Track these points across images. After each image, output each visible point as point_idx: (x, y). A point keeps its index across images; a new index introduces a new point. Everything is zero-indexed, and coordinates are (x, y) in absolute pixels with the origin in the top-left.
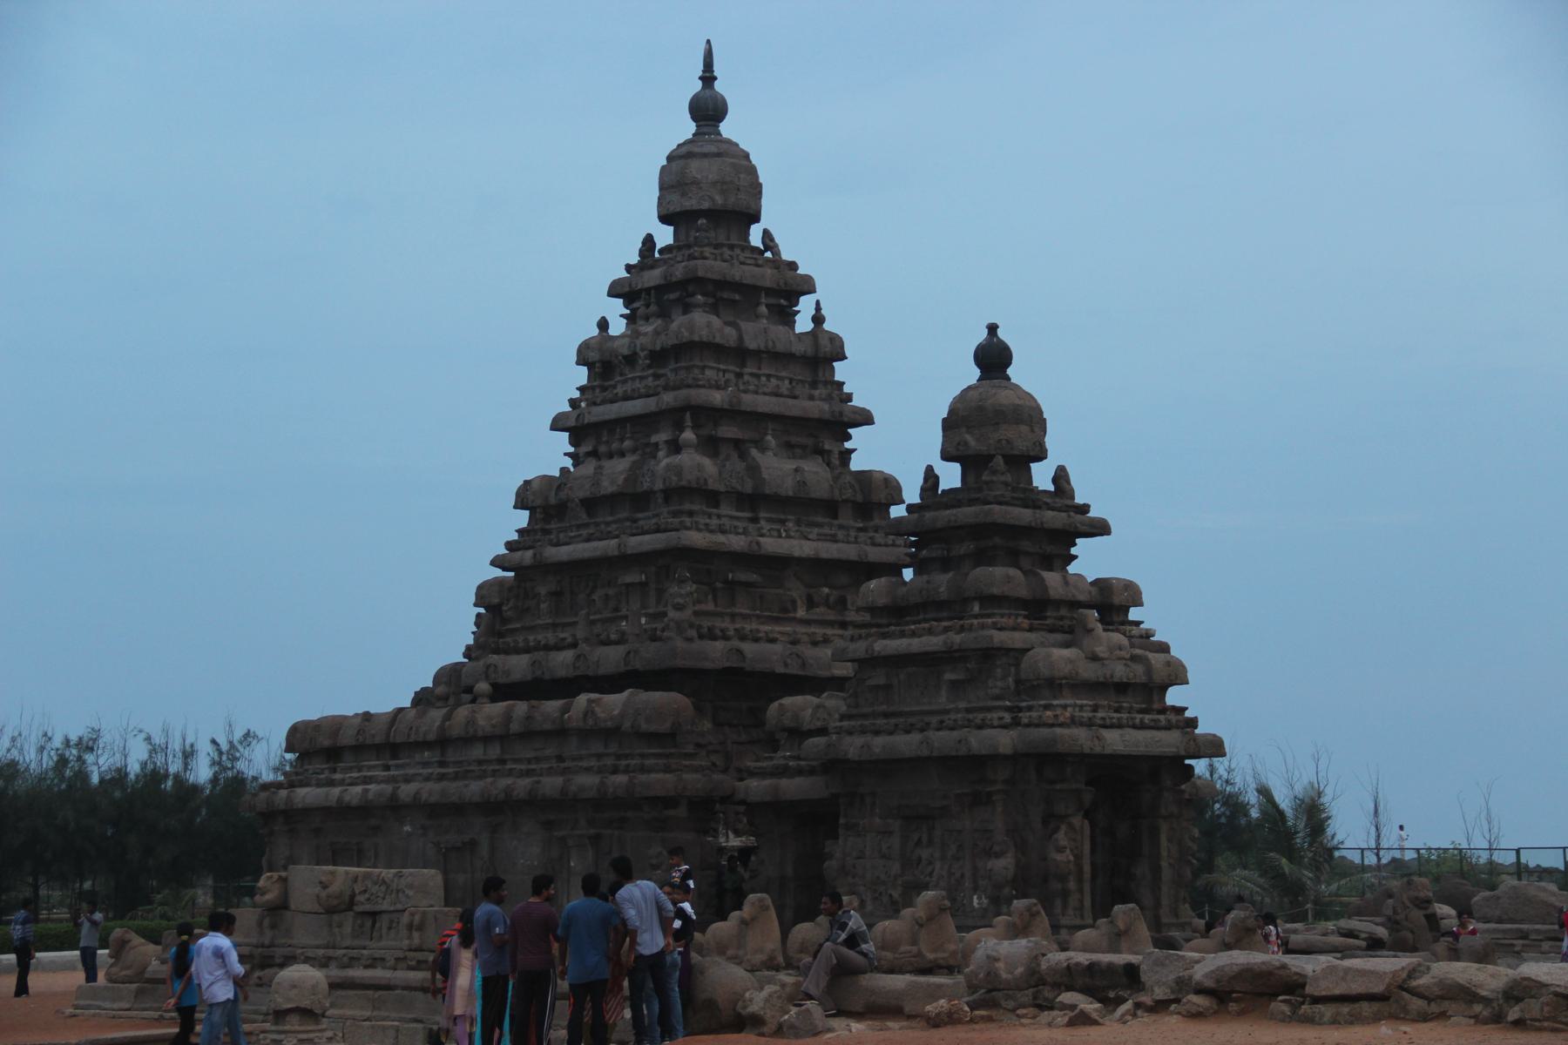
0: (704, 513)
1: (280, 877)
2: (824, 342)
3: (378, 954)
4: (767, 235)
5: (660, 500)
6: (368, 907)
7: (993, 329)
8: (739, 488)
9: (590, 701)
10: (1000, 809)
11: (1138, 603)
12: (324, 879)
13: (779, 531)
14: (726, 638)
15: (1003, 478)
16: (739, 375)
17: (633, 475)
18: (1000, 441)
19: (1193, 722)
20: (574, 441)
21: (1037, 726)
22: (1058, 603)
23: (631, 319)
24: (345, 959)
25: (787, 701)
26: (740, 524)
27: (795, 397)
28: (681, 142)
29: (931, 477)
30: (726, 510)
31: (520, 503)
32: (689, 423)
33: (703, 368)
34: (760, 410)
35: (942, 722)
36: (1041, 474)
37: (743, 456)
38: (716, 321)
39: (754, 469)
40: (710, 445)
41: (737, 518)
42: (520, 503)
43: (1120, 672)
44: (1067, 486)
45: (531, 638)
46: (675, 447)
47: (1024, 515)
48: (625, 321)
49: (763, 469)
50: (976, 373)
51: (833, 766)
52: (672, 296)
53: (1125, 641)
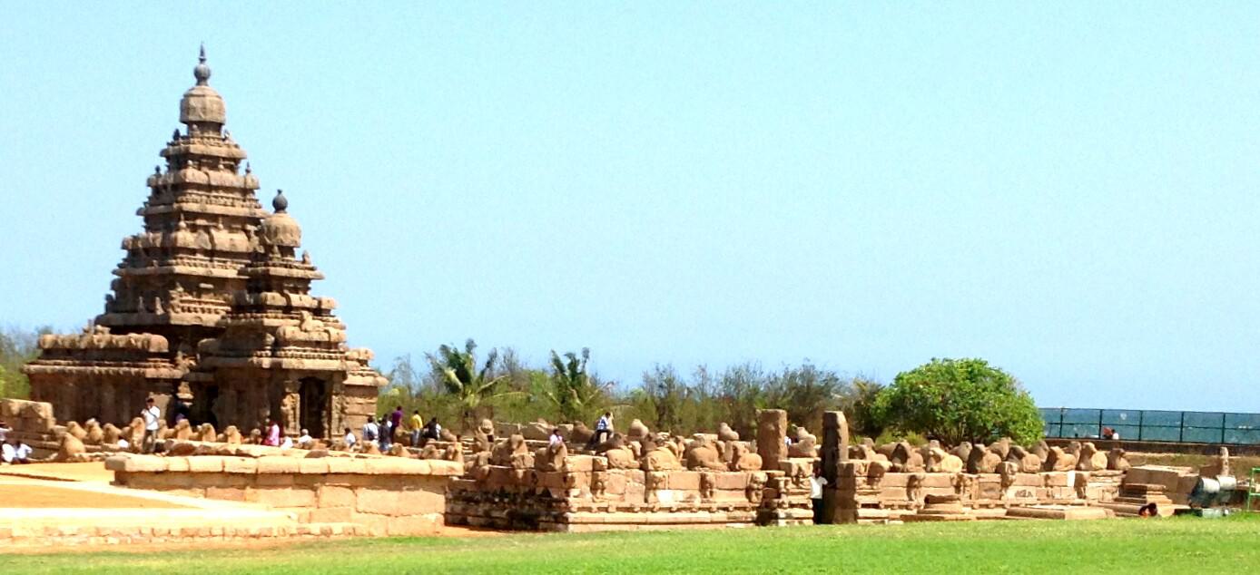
2: (249, 181)
7: (280, 192)
12: (10, 404)
15: (276, 255)
16: (208, 196)
20: (146, 220)
22: (297, 308)
25: (205, 340)
26: (204, 263)
31: (124, 247)
37: (209, 233)
39: (212, 239)
40: (194, 229)
42: (124, 247)
43: (315, 337)
46: (178, 229)
47: (283, 272)
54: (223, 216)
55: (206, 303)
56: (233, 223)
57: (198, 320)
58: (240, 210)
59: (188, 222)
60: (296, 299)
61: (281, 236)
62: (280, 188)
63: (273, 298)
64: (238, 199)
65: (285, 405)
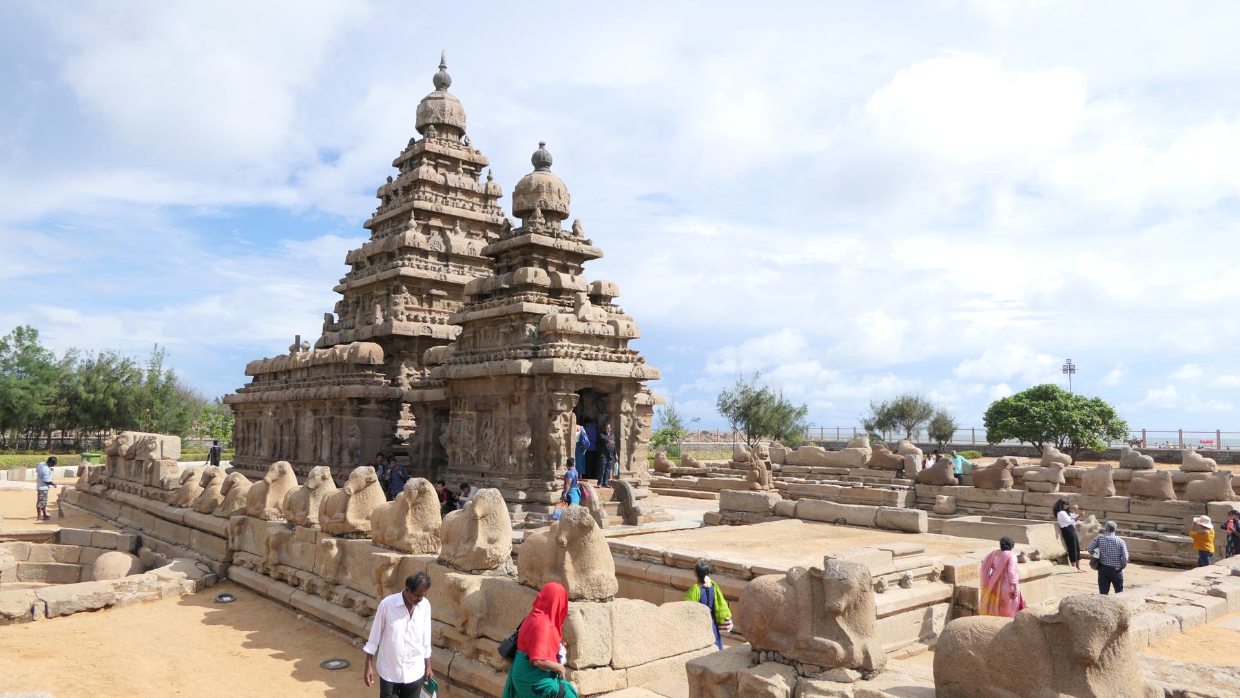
0: (417, 260)
2: (491, 186)
5: (397, 252)
7: (542, 145)
8: (439, 250)
10: (524, 406)
13: (459, 272)
14: (424, 321)
17: (388, 244)
18: (540, 202)
19: (640, 360)
21: (547, 357)
26: (437, 267)
27: (474, 211)
30: (431, 259)
31: (348, 263)
32: (413, 216)
33: (424, 192)
34: (453, 214)
36: (565, 226)
38: (432, 170)
39: (447, 241)
40: (427, 230)
41: (438, 264)
42: (348, 263)
43: (598, 329)
44: (578, 229)
46: (407, 228)
47: (548, 241)
49: (451, 241)
50: (533, 168)
51: (447, 382)
53: (605, 314)
54: (462, 219)
55: (439, 312)
56: (472, 226)
58: (479, 215)
59: (420, 222)
60: (566, 280)
61: (544, 196)
63: (537, 274)
64: (477, 205)
65: (555, 431)
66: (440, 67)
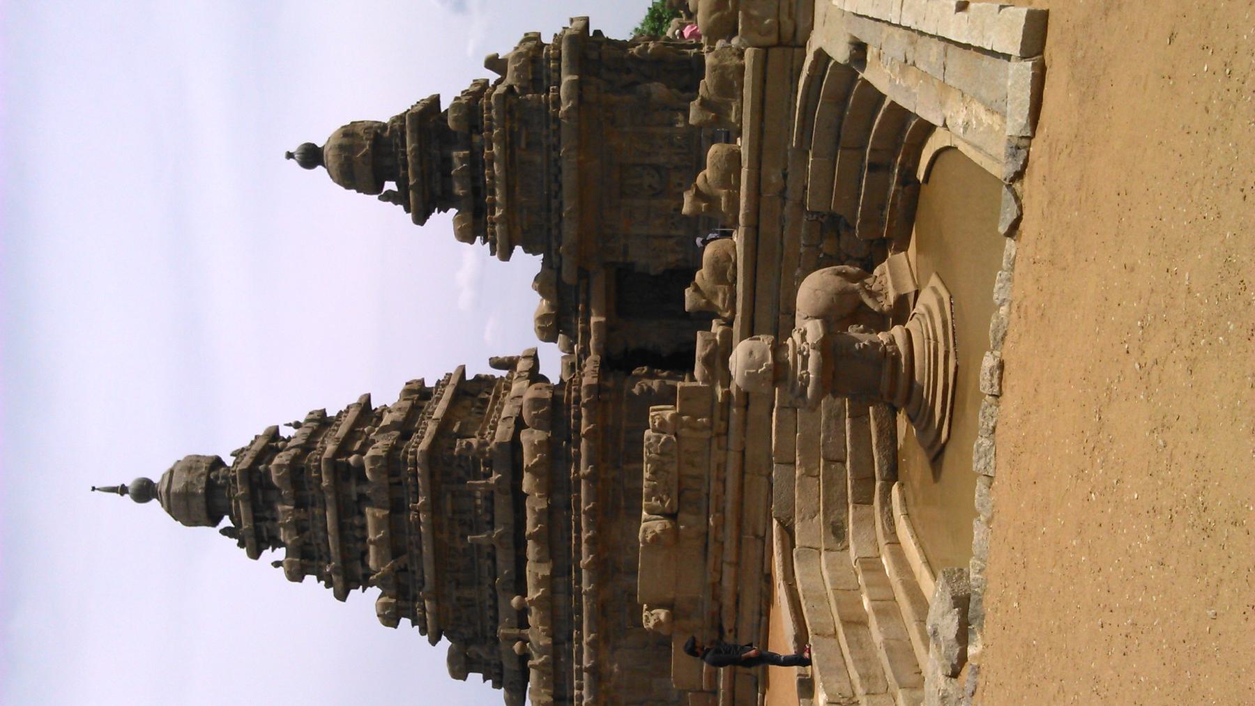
1: (646, 610)
3: (714, 474)
4: (232, 455)
5: (395, 480)
6: (675, 494)
7: (290, 155)
9: (528, 469)
11: (488, 81)
14: (494, 434)
23: (276, 544)
24: (718, 515)
28: (160, 505)
29: (389, 197)
32: (344, 459)
33: (310, 461)
35: (554, 150)
39: (385, 430)
45: (489, 602)
48: (277, 549)
50: (320, 168)
52: (260, 497)
57: (508, 420)
62: (284, 155)
66: (122, 495)
